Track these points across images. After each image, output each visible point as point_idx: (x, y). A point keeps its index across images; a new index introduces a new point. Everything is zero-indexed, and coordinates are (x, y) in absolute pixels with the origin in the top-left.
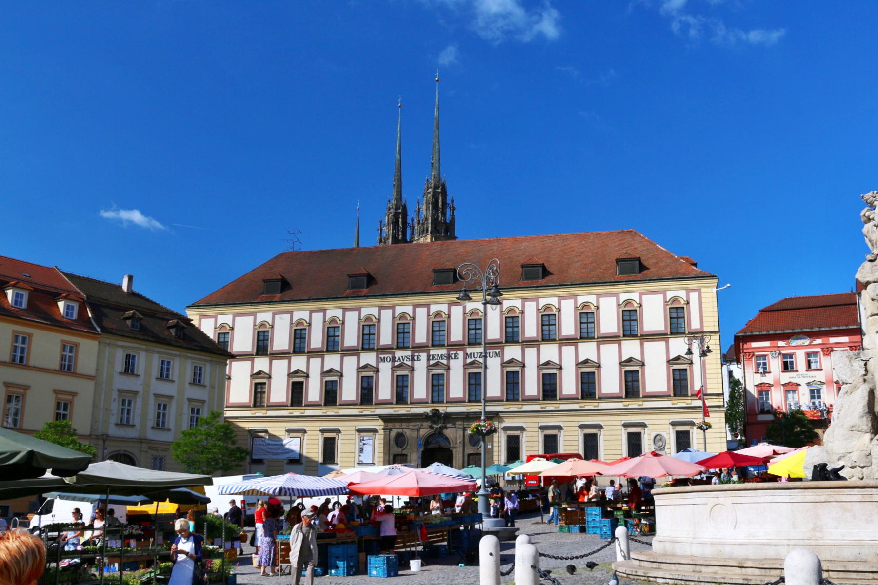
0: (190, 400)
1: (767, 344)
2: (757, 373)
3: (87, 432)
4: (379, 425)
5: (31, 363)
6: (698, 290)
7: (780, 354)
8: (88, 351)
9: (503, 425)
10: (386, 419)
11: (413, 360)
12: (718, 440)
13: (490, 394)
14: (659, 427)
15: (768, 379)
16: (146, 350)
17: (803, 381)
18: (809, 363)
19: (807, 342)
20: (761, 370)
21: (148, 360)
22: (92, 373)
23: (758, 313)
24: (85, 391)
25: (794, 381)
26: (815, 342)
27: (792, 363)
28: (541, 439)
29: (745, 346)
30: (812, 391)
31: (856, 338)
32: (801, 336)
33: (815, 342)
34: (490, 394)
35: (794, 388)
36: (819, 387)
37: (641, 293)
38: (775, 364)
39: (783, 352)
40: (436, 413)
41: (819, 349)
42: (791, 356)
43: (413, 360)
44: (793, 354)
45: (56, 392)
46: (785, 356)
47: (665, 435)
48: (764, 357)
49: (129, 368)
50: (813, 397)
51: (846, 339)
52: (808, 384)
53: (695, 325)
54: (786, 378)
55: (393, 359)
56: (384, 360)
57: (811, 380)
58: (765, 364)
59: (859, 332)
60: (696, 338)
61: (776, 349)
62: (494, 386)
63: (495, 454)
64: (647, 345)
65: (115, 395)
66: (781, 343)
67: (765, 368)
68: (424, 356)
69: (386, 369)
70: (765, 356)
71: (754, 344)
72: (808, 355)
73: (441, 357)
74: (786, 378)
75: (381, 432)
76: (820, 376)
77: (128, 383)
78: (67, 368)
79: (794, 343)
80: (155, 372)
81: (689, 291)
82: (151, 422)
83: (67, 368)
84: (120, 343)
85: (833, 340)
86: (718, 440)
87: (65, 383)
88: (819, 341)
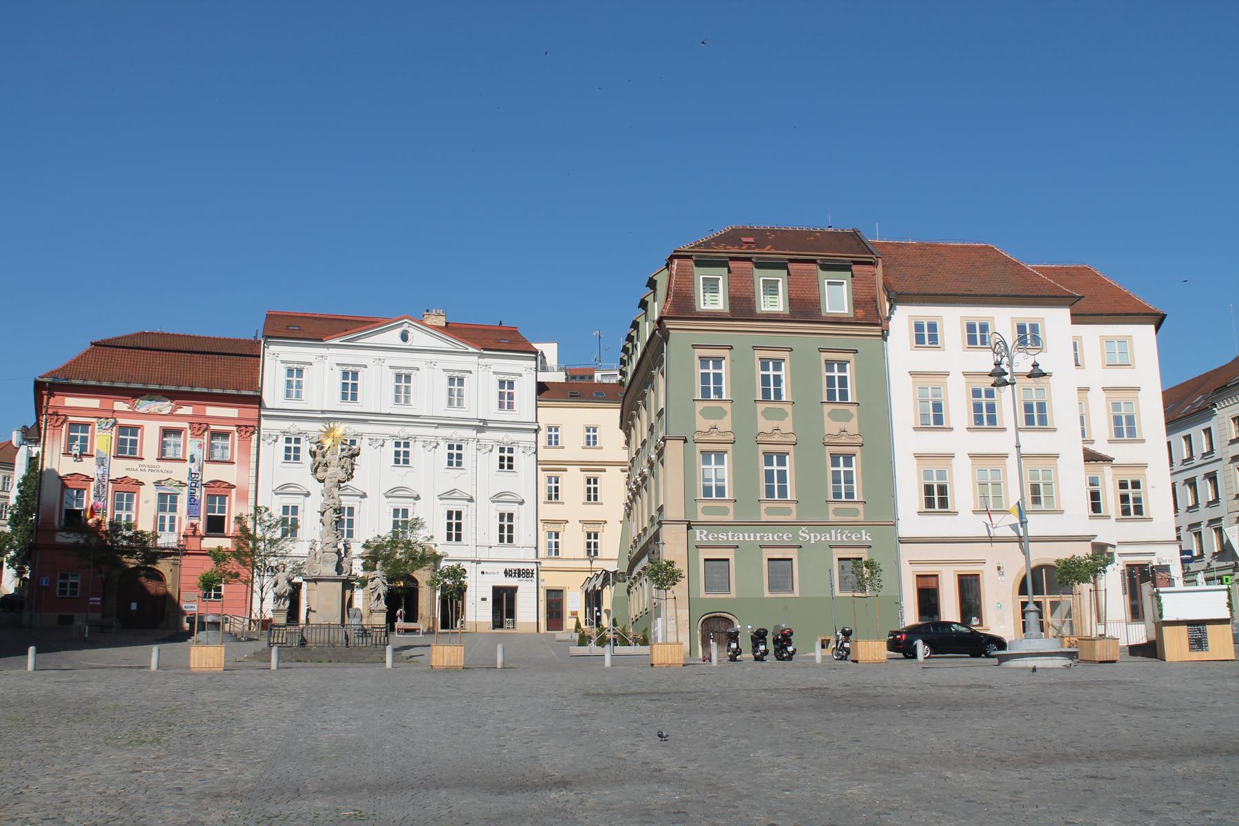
1: (94, 403)
2: (66, 454)
7: (114, 424)
15: (88, 467)
17: (148, 478)
18: (163, 445)
19: (165, 407)
20: (76, 450)
23: (88, 346)
25: (133, 475)
26: (179, 412)
27: (134, 443)
29: (53, 401)
30: (162, 497)
31: (251, 412)
32: (159, 396)
33: (179, 412)
35: (131, 488)
36: (176, 490)
38: (102, 440)
39: (121, 421)
41: (186, 425)
42: (134, 430)
44: (138, 427)
46: (123, 429)
48: (85, 426)
50: (162, 508)
51: (232, 412)
52: (158, 484)
54: (119, 468)
57: (163, 477)
58: (84, 439)
59: (257, 401)
61: (109, 414)
66: (120, 406)
67: (83, 448)
70: (88, 424)
71: (71, 401)
72: (166, 432)
74: (119, 468)
76: (180, 472)
79: (144, 406)
85: (212, 411)
88: (187, 410)
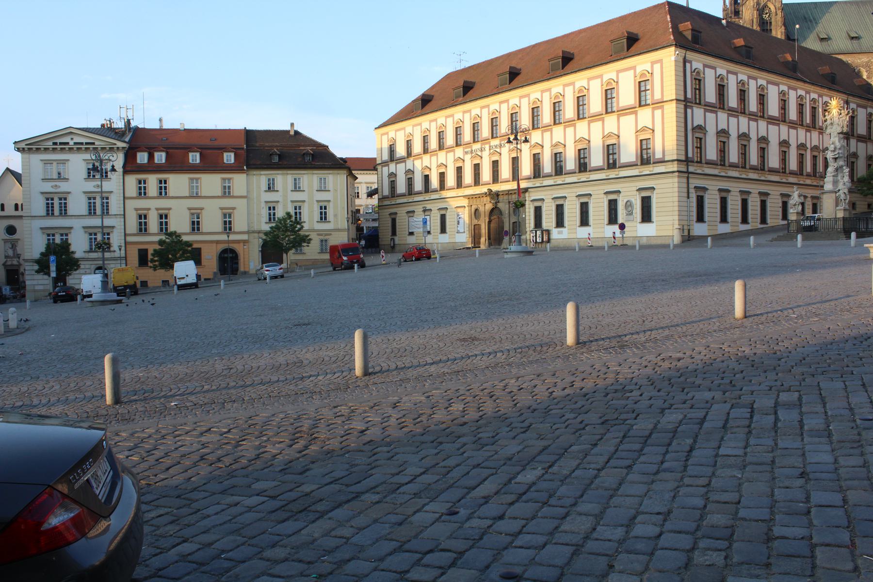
0: (318, 201)
3: (246, 229)
4: (465, 202)
5: (203, 195)
6: (660, 61)
8: (239, 181)
9: (533, 198)
10: (469, 197)
11: (481, 151)
12: (671, 204)
13: (546, 171)
14: (629, 195)
16: (282, 174)
21: (284, 179)
22: (245, 194)
24: (240, 206)
28: (554, 208)
34: (546, 171)
37: (618, 72)
40: (490, 190)
43: (481, 151)
45: (221, 209)
47: (633, 200)
49: (270, 188)
53: (657, 96)
55: (471, 152)
56: (466, 153)
60: (658, 108)
62: (526, 169)
63: (527, 222)
64: (621, 118)
65: (263, 205)
68: (487, 146)
69: (468, 158)
73: (496, 146)
75: (467, 208)
77: (272, 197)
78: (227, 192)
80: (291, 186)
81: (653, 63)
82: (317, 216)
83: (227, 192)
84: (263, 172)
86: (671, 204)
87: (227, 203)
